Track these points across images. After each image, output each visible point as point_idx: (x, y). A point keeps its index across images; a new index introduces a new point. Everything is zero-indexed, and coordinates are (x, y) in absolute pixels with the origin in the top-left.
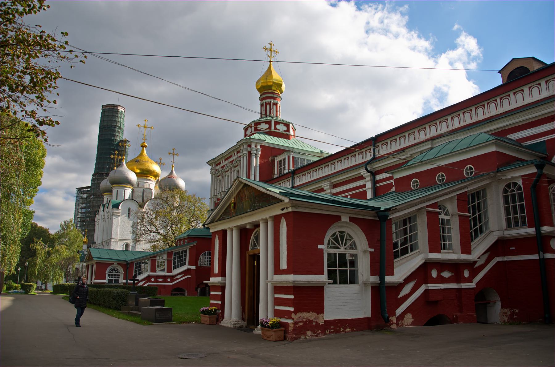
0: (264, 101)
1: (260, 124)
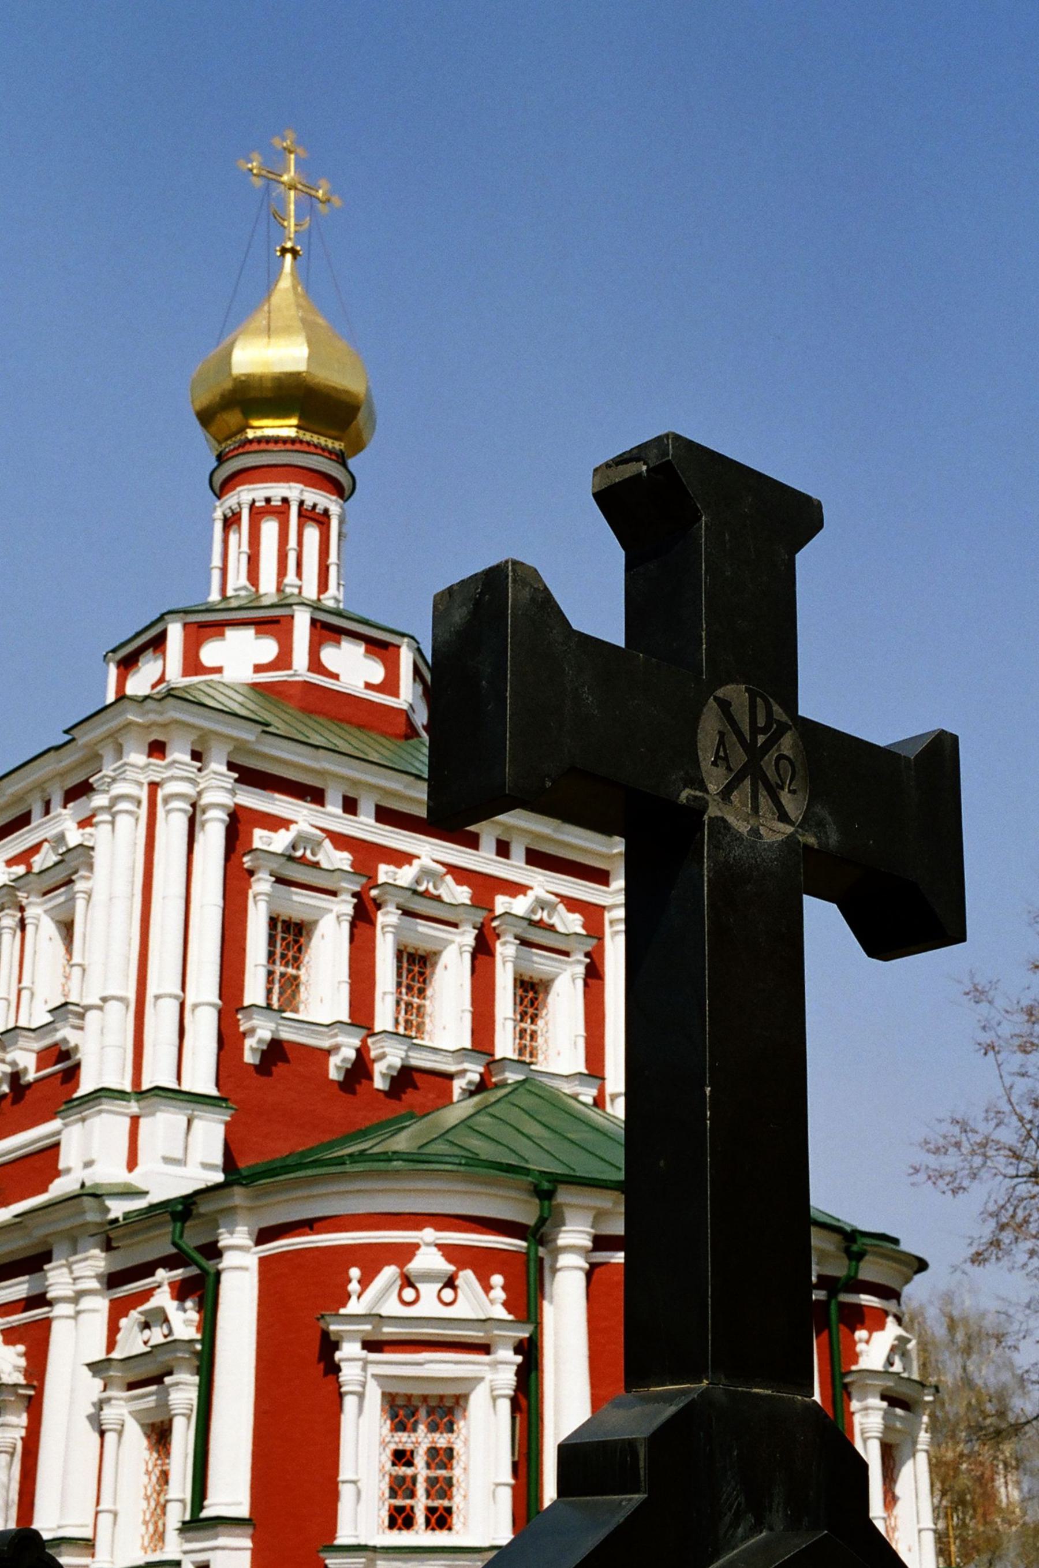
0: (246, 495)
1: (222, 635)
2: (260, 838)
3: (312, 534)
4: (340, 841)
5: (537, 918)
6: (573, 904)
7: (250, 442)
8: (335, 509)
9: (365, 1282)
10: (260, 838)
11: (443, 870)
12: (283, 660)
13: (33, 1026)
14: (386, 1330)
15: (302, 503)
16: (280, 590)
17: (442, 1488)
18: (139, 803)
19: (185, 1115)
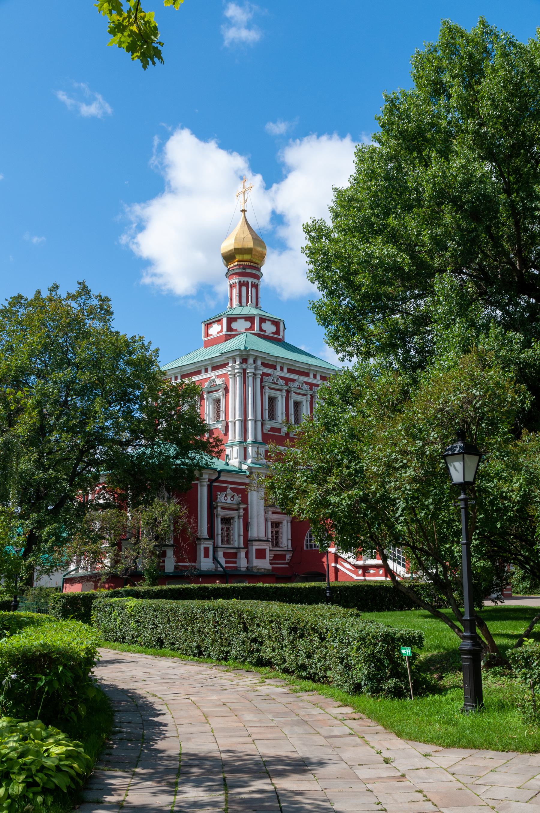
2: (266, 378)
3: (254, 290)
4: (282, 378)
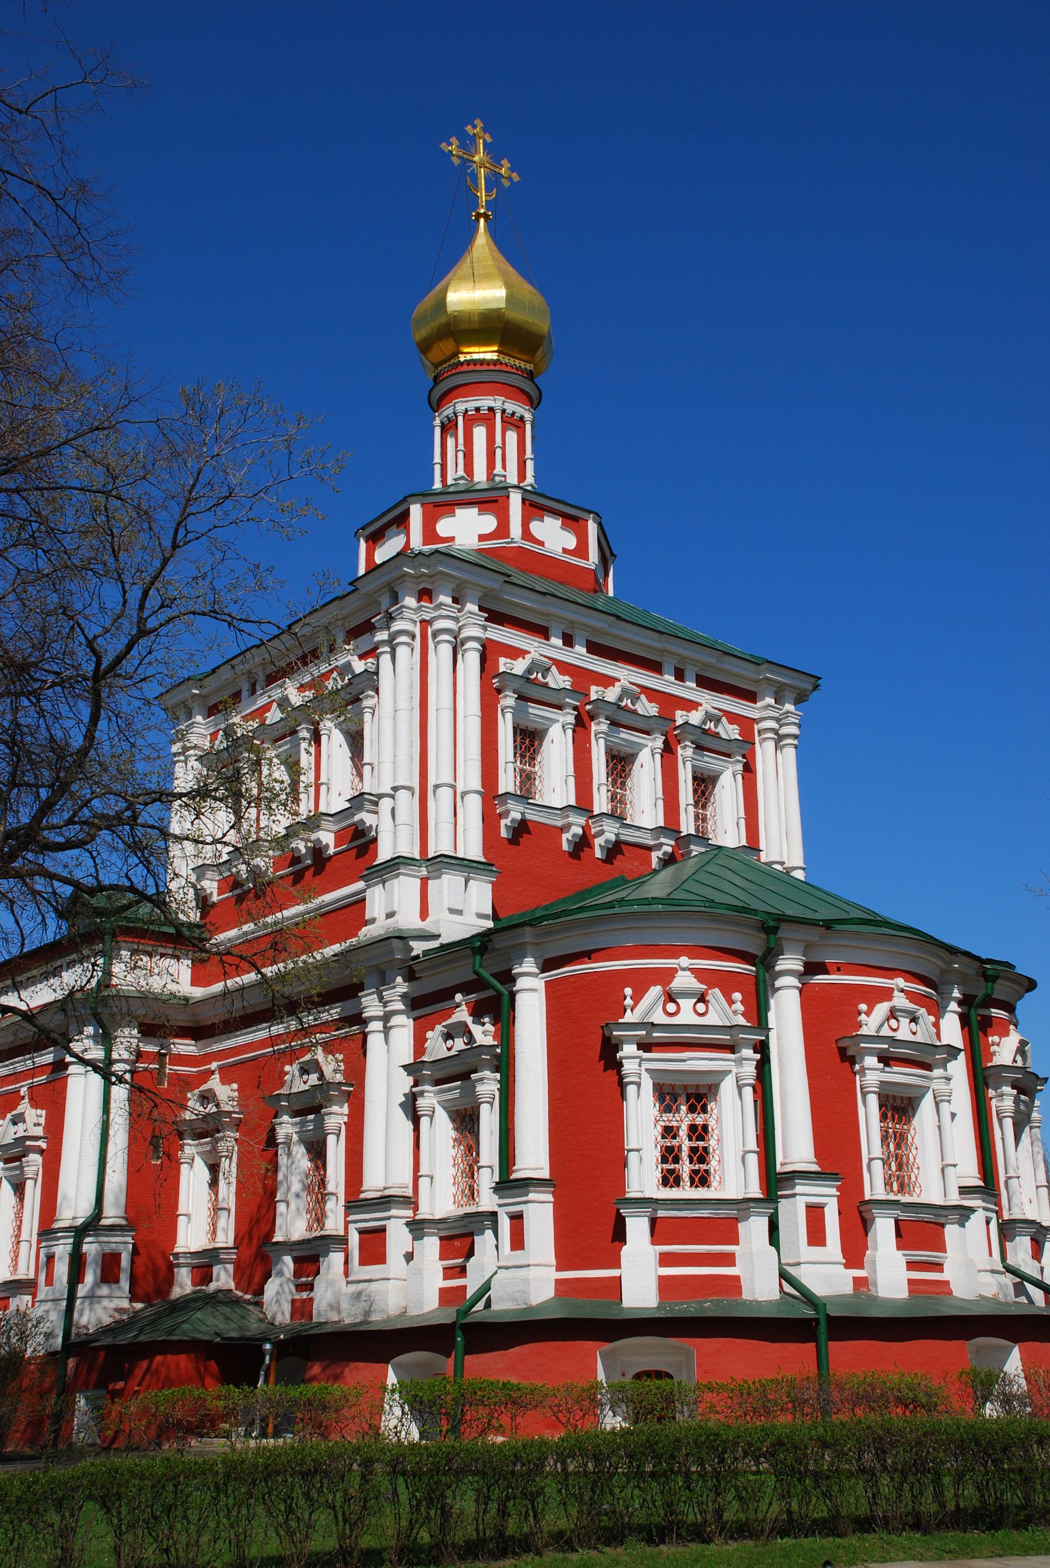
2: (504, 664)
3: (512, 436)
4: (564, 668)
5: (707, 727)
6: (733, 718)
7: (461, 364)
8: (528, 416)
9: (637, 998)
10: (504, 664)
11: (639, 690)
12: (502, 530)
13: (332, 813)
14: (655, 1035)
15: (504, 411)
16: (491, 476)
17: (700, 1155)
18: (413, 637)
19: (463, 876)
